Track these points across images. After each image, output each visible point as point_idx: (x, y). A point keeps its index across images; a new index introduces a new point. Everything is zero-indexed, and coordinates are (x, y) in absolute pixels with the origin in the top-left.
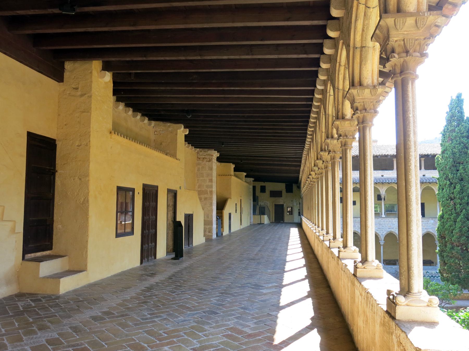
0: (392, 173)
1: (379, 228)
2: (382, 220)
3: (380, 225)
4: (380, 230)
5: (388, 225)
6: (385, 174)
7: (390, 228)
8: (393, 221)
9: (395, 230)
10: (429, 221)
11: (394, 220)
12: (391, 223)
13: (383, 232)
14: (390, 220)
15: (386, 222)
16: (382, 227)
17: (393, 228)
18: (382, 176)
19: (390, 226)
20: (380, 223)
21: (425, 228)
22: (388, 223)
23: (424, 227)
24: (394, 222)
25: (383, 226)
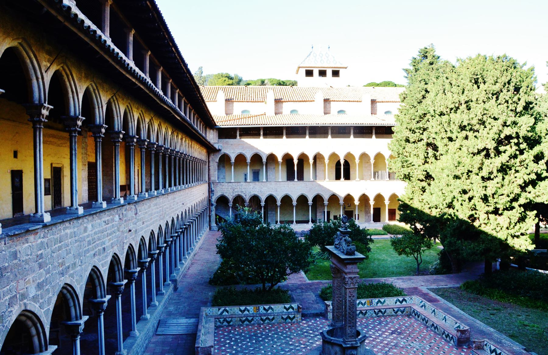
23: (110, 240)
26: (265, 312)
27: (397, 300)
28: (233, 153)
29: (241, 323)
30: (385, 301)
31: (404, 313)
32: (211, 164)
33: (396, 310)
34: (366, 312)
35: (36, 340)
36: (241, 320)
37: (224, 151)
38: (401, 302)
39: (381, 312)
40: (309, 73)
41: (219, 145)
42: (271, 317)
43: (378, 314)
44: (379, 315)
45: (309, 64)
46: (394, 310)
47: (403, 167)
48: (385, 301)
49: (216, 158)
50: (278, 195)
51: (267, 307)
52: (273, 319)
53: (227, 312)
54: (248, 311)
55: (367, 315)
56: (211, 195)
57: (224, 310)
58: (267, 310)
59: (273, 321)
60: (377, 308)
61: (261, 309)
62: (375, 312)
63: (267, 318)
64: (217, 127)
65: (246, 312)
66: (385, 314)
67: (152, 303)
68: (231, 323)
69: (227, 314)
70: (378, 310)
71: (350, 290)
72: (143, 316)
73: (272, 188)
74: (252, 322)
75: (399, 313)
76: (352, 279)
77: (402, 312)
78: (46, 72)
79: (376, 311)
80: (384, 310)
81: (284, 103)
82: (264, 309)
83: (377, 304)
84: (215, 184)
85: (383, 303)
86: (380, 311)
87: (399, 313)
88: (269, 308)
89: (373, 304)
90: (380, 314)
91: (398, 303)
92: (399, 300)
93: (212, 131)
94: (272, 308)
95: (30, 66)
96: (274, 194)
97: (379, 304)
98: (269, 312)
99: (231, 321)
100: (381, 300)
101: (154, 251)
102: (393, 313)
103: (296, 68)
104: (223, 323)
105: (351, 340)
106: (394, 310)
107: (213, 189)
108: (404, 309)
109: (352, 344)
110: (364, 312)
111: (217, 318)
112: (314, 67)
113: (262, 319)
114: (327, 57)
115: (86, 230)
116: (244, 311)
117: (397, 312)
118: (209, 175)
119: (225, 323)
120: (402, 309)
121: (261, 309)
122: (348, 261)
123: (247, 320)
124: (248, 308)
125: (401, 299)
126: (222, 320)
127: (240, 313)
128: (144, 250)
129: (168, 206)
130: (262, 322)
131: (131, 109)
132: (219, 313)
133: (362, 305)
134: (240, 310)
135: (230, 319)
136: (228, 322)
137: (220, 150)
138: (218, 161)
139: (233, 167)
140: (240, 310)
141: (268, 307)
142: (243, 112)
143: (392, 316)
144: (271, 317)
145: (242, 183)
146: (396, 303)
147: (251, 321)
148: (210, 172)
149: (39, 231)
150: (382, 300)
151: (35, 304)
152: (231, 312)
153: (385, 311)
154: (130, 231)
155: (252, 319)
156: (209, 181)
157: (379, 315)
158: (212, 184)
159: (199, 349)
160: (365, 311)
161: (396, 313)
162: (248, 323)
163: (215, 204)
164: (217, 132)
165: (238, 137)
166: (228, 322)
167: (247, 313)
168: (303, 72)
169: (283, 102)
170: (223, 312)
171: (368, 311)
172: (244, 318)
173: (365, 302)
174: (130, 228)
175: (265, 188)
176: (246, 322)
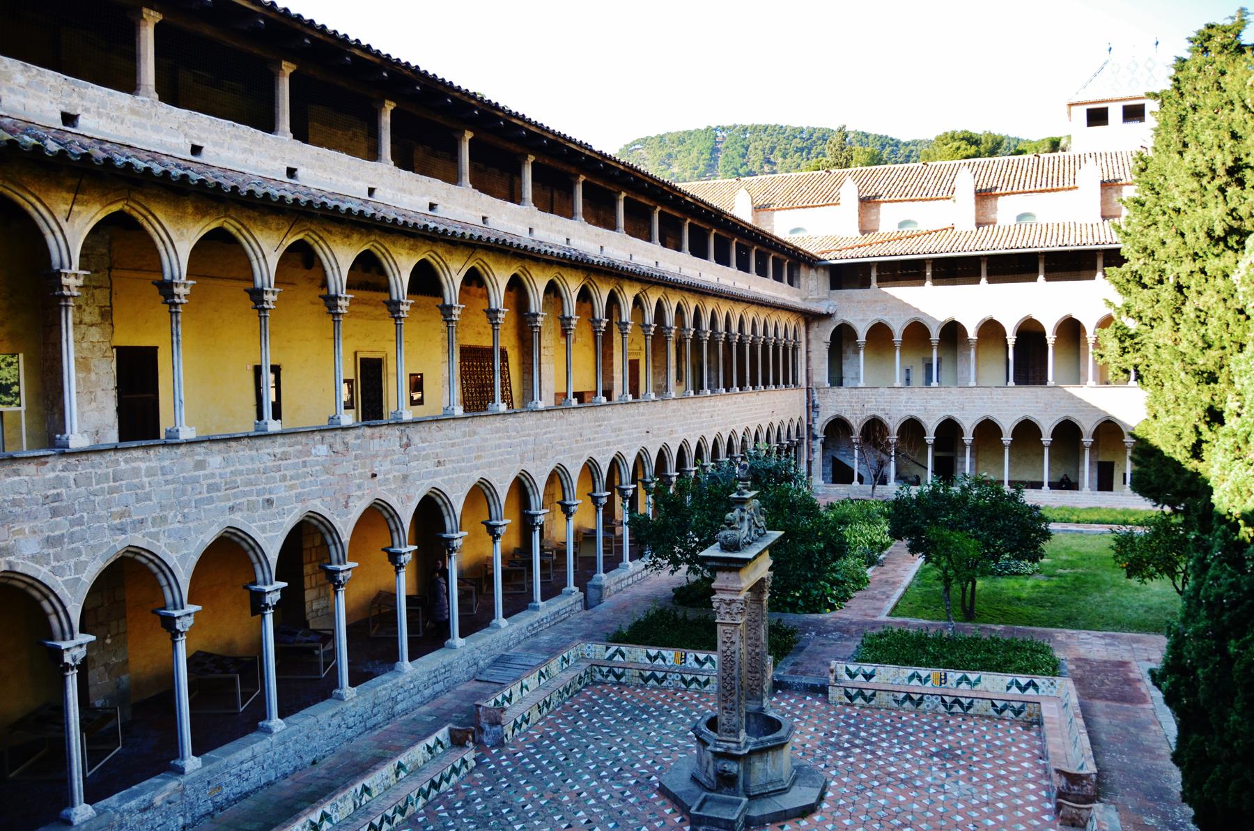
0: (133, 111)
1: (50, 542)
2: (72, 475)
3: (55, 513)
4: (57, 558)
5: (108, 504)
6: (87, 110)
7: (122, 530)
8: (136, 472)
9: (151, 535)
10: (308, 453)
11: (143, 465)
12: (129, 487)
13: (80, 567)
14: (123, 466)
15: (95, 487)
16: (73, 523)
17: (142, 522)
18: (69, 119)
19: (122, 515)
20: (58, 497)
21: (293, 492)
22: (112, 491)
23: (292, 487)
24: (146, 480)
25: (80, 522)
26: (696, 666)
27: (1012, 683)
28: (862, 320)
29: (641, 682)
30: (979, 680)
31: (1022, 715)
32: (812, 347)
33: (999, 704)
34: (921, 699)
35: (53, 619)
36: (641, 676)
37: (842, 317)
38: (1023, 689)
39: (961, 705)
40: (1097, 117)
41: (830, 302)
42: (702, 679)
43: (951, 707)
44: (953, 710)
45: (1096, 94)
46: (993, 705)
47: (1124, 351)
48: (979, 680)
49: (824, 334)
50: (967, 419)
51: (702, 656)
52: (707, 683)
53: (623, 655)
54: (664, 660)
55: (923, 706)
56: (813, 415)
57: (617, 651)
58: (701, 663)
59: (707, 688)
60: (952, 692)
61: (690, 659)
62: (943, 701)
63: (695, 680)
64: (823, 263)
65: (659, 662)
66: (971, 711)
67: (494, 621)
68: (623, 680)
69: (621, 659)
70: (954, 698)
71: (724, 628)
72: (450, 641)
73: (953, 403)
74: (664, 684)
75: (1008, 714)
76: (729, 604)
77: (1018, 712)
78: (67, 220)
79: (946, 698)
80: (969, 700)
81: (1000, 198)
82: (697, 659)
83: (959, 683)
84: (822, 391)
85: (975, 684)
86: (957, 701)
87: (1008, 714)
88: (708, 659)
89: (948, 683)
90: (957, 708)
91: (1014, 690)
92: (1018, 683)
93: (812, 272)
94: (712, 660)
95: (35, 215)
96: (956, 416)
97: (964, 685)
98: (705, 667)
99: (623, 674)
100: (969, 675)
101: (497, 519)
102: (992, 712)
103: (1066, 108)
104: (607, 676)
105: (729, 739)
106: (993, 705)
107: (816, 402)
108: (1023, 707)
109: (729, 748)
110: (916, 697)
111: (598, 666)
112: (1111, 101)
113: (683, 680)
114: (1150, 70)
115: (200, 465)
116: (656, 658)
117: (1002, 711)
118: (807, 371)
119: (611, 678)
120: (1017, 705)
121: (690, 659)
122: (718, 564)
123: (653, 676)
124: (664, 653)
125: (1023, 680)
126: (605, 670)
127: (648, 661)
128: (449, 515)
129: (566, 434)
130: (683, 686)
131: (387, 250)
132: (607, 655)
133: (920, 680)
134: (649, 656)
135: (621, 670)
136: (618, 677)
137: (828, 316)
138: (828, 340)
139: (862, 353)
140: (649, 656)
141: (705, 655)
142: (902, 225)
143: (989, 717)
144: (702, 679)
145: (881, 390)
146: (1008, 688)
147: (662, 681)
148: (810, 363)
149: (50, 459)
150: (973, 677)
151: (37, 566)
152: (630, 658)
153: (971, 704)
154: (374, 475)
155: (665, 678)
156: (808, 384)
157: (953, 710)
158: (815, 391)
159: (481, 709)
160: (919, 696)
161: (1000, 711)
162: (655, 683)
163: (821, 436)
164: (827, 274)
165: (874, 284)
166: (618, 677)
167: (661, 662)
168: (1081, 114)
169: (997, 196)
170: (614, 655)
171: (925, 697)
172: (648, 673)
173: (929, 676)
174: (376, 470)
175: (937, 402)
176: (652, 682)
